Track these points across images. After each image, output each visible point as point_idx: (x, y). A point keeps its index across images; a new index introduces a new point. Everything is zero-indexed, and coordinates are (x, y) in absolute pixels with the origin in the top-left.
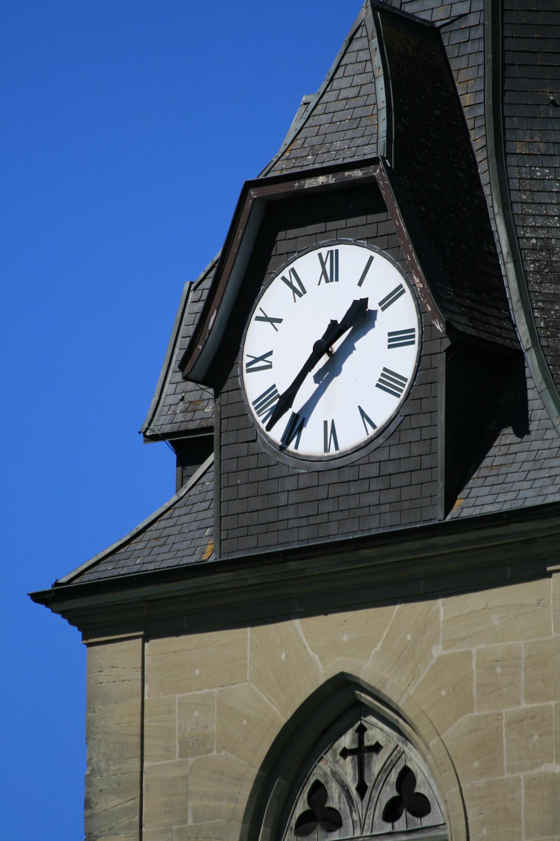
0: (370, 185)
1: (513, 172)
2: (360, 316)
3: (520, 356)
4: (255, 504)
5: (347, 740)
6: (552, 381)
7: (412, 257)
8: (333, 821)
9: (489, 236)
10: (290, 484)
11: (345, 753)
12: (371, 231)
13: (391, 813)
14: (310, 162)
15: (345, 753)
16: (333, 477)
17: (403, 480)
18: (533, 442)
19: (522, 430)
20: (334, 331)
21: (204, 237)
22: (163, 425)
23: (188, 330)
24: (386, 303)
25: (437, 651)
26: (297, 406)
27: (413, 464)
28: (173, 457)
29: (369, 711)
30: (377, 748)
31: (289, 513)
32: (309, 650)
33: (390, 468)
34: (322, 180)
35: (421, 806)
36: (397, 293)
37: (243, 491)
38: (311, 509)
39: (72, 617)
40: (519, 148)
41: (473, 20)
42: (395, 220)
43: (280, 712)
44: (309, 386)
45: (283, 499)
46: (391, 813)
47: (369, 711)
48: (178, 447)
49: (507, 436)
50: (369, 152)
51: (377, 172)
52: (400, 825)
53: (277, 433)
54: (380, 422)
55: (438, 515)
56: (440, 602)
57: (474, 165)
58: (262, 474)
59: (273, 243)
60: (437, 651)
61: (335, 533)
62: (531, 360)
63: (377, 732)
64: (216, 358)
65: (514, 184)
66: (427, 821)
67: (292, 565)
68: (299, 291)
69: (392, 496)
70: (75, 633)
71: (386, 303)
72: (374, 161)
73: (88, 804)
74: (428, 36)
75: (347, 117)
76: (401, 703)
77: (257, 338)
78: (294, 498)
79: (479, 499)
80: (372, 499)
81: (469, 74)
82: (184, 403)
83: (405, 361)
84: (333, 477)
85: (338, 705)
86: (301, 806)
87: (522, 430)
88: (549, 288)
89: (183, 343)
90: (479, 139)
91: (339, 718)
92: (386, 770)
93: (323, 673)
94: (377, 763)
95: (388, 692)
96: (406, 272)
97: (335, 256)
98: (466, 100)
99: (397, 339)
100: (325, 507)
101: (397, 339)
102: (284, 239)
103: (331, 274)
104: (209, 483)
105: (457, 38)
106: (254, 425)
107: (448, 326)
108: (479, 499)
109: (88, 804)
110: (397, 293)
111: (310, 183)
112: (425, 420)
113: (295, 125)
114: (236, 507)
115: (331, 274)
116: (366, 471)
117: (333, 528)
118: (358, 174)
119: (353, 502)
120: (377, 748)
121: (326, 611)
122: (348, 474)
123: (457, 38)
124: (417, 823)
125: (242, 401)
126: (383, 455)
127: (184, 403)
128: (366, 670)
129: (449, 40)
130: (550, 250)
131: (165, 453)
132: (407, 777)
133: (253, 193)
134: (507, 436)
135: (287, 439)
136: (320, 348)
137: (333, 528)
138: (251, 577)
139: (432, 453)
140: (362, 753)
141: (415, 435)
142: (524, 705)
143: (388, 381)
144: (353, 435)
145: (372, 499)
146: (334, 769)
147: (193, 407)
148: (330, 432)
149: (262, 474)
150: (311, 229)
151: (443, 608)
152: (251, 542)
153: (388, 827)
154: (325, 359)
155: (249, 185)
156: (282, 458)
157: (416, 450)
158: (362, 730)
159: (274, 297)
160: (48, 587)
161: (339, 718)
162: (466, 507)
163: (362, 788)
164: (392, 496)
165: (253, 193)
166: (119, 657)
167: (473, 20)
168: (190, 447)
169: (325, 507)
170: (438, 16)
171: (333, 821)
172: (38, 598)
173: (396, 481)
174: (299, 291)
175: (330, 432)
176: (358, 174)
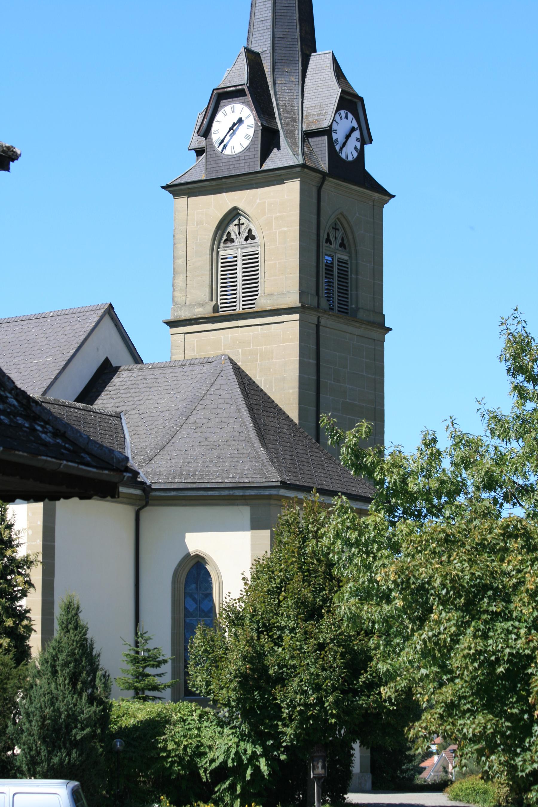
0: (243, 91)
1: (277, 87)
2: (240, 121)
3: (278, 131)
4: (214, 166)
5: (236, 222)
6: (286, 137)
7: (253, 107)
8: (232, 241)
9: (271, 102)
10: (223, 161)
11: (235, 225)
12: (243, 101)
13: (246, 239)
14: (229, 85)
15: (235, 225)
16: (233, 160)
17: (250, 160)
18: (281, 151)
19: (279, 149)
20: (234, 124)
21: (203, 101)
22: (193, 147)
23: (199, 124)
24: (247, 118)
25: (258, 201)
26: (225, 143)
27: (253, 156)
28: (195, 154)
29: (241, 215)
30: (243, 224)
31: (223, 168)
32: (225, 201)
33: (247, 157)
34: (231, 89)
35: (253, 238)
36: (249, 116)
37: (212, 163)
38: (228, 167)
39: (171, 192)
40: (279, 82)
41: (268, 52)
42: (249, 98)
43: (220, 215)
44: (228, 138)
45: (221, 165)
46: (246, 239)
47: (241, 215)
48: (196, 152)
49: (275, 150)
50: (243, 82)
51: (245, 87)
52: (248, 242)
53: (220, 149)
54: (245, 147)
55: (258, 169)
56: (259, 189)
57: (268, 86)
58: (216, 158)
59: (219, 103)
60: (258, 201)
61: (234, 173)
62: (281, 132)
63: (243, 220)
64: (205, 132)
65: (277, 90)
66: (254, 241)
67: (223, 180)
68: (226, 115)
69: (248, 164)
70: (171, 196)
71: (247, 118)
72: (244, 84)
73: (174, 236)
74: (257, 55)
75: (239, 75)
76: (249, 213)
77: (215, 126)
78: (224, 164)
79: (268, 165)
80: (243, 165)
81: (267, 64)
82: (199, 142)
83: (251, 132)
84: (233, 160)
85: (234, 214)
86: (225, 237)
87: (279, 149)
88: (286, 115)
89: (198, 127)
90: (269, 80)
91: (234, 217)
92: (245, 229)
93: (230, 206)
94: (243, 227)
95: (246, 211)
96: (252, 111)
97: (234, 107)
98: (266, 70)
99: (249, 127)
100: (231, 167)
101: (249, 127)
102: (222, 102)
103: (233, 111)
104: (204, 161)
105: (264, 56)
106: (214, 147)
107: (262, 124)
108: (268, 165)
109: (174, 236)
110: (249, 116)
111: (229, 89)
112: (256, 146)
113: (225, 76)
114: (210, 166)
115: (233, 111)
116: (241, 158)
117: (233, 172)
118: (240, 87)
119: (238, 165)
120: (243, 224)
121: (231, 191)
122: (237, 159)
123: (264, 56)
124: (253, 241)
125: (212, 141)
126: (245, 154)
127: (199, 142)
128: (240, 206)
129: (262, 56)
130: (286, 106)
131: (193, 153)
132: (250, 231)
133: (215, 92)
134: (275, 150)
135: (223, 150)
136: (231, 129)
137: (233, 172)
138: (214, 183)
139: (257, 154)
140: (239, 225)
141: (253, 150)
142: (278, 214)
143: (247, 137)
144: (238, 150)
145: (243, 165)
146: (233, 229)
147: (200, 142)
148: (233, 148)
149: (216, 158)
150: (229, 100)
151: (259, 191)
152: (218, 174)
153: (245, 242)
154: (232, 131)
155: (214, 90)
156: (221, 155)
157: (253, 153)
158: (239, 220)
159: (219, 116)
160: (165, 185)
161: (234, 217)
162: (265, 167)
163: (239, 233)
164: (248, 164)
165: (215, 92)
166: (182, 201)
167: (268, 52)
168: (199, 152)
169: (231, 167)
170: (259, 51)
171: (232, 241)
172: (163, 187)
173: (249, 161)
174: (226, 115)
175: (233, 148)
176: (240, 87)
